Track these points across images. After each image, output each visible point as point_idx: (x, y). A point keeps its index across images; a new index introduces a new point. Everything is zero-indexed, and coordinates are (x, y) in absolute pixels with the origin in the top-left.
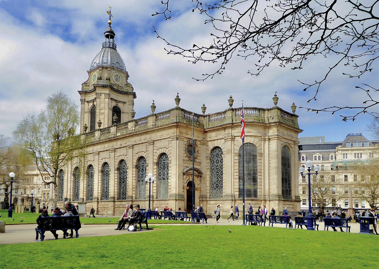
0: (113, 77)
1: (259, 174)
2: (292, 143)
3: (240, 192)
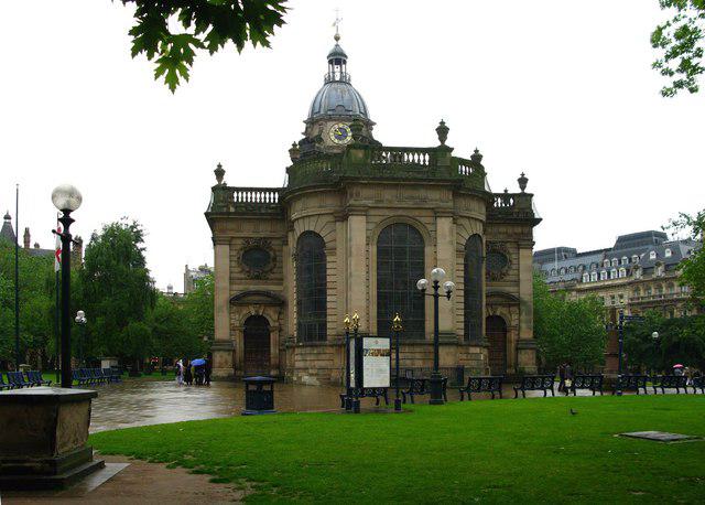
1: (329, 292)
2: (430, 213)
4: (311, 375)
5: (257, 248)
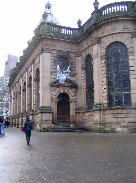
1: (131, 76)
3: (109, 100)
4: (123, 127)
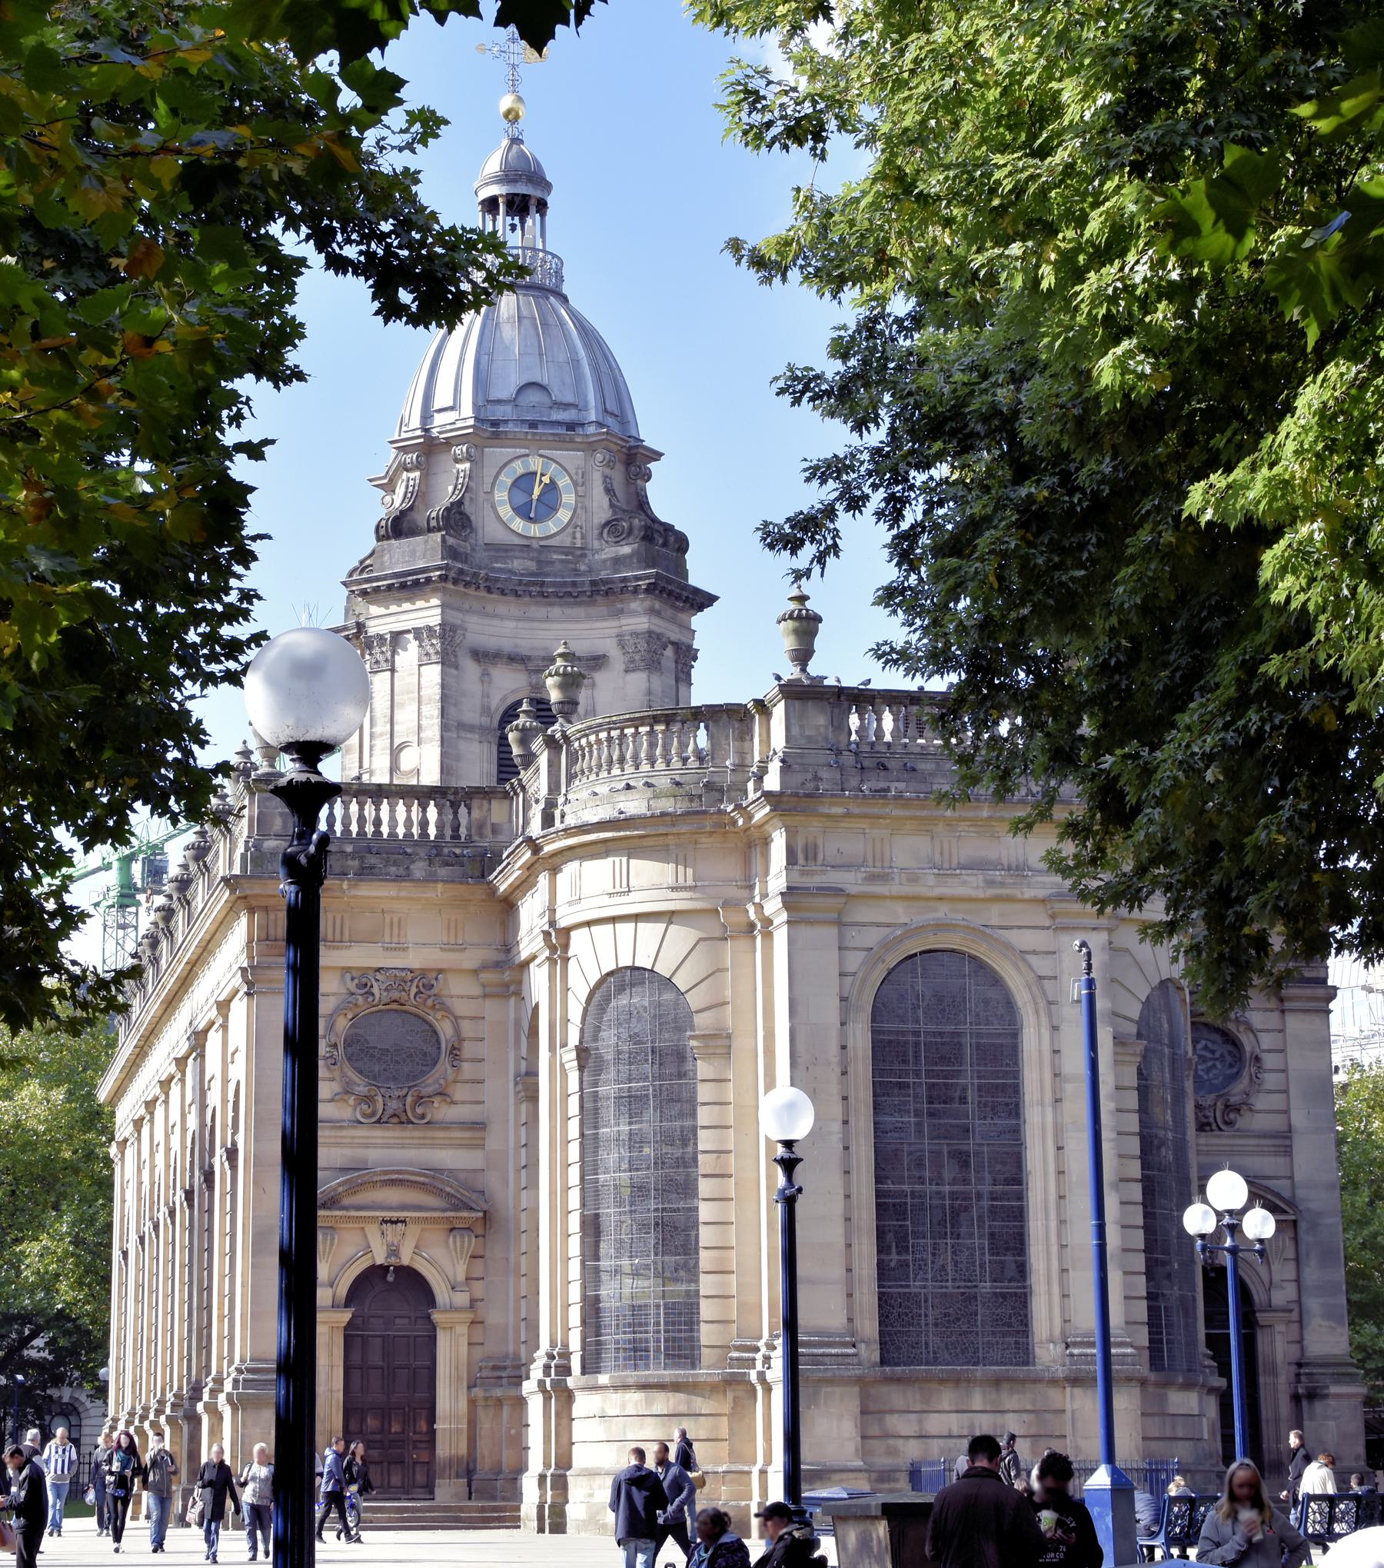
0: (501, 495)
1: (705, 1187)
5: (396, 1008)
